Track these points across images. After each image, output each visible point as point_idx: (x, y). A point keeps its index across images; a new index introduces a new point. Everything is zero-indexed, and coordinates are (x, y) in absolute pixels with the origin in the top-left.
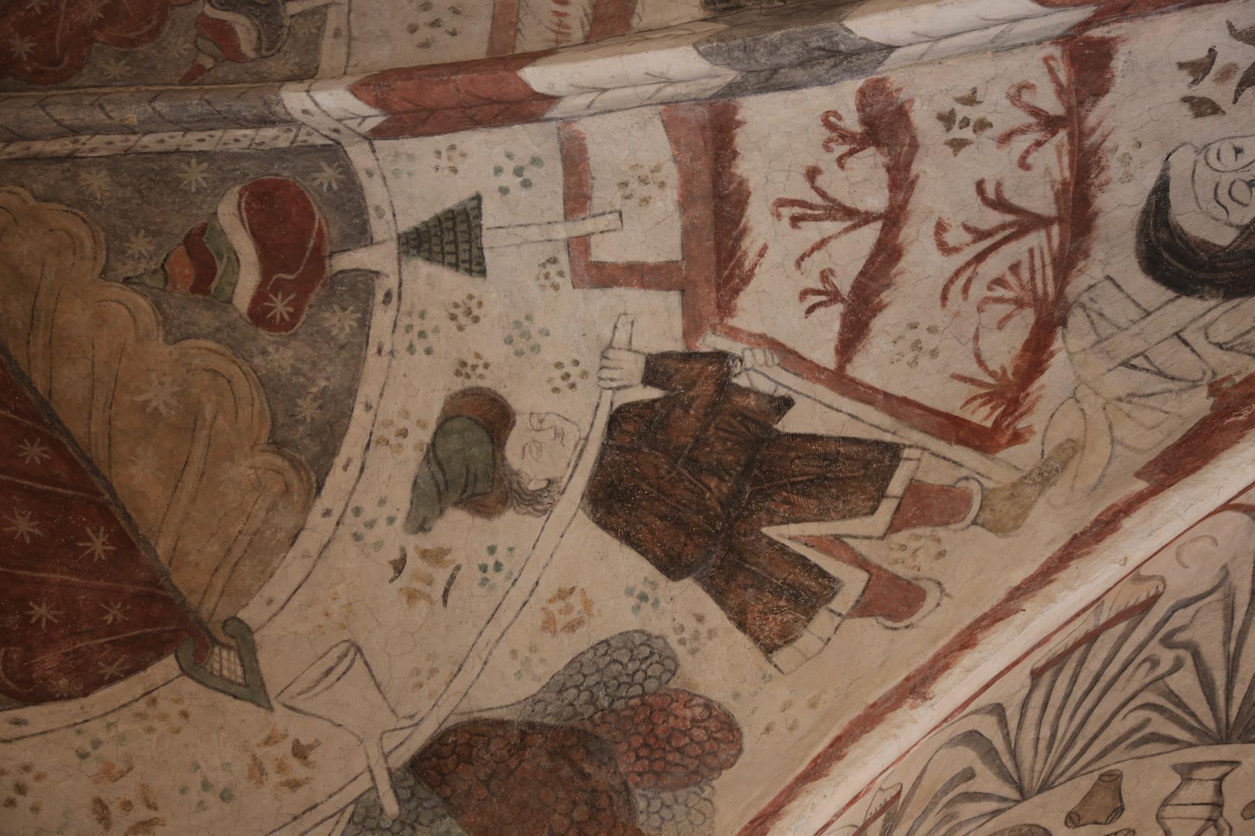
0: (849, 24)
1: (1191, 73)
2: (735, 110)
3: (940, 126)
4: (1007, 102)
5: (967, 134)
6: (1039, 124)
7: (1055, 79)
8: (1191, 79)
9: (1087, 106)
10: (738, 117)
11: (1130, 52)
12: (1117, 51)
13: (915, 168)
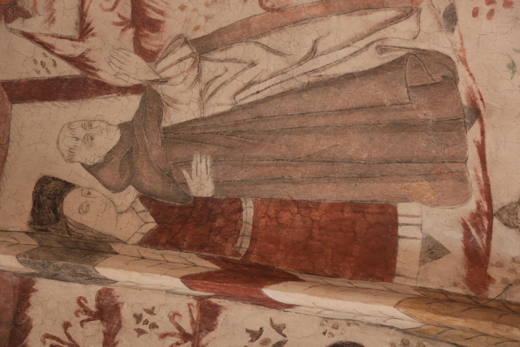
0: (97, 269)
1: (251, 336)
2: (33, 283)
3: (133, 320)
4: (167, 319)
5: (146, 328)
6: (180, 334)
7: (191, 316)
8: (250, 339)
9: (203, 334)
10: (34, 287)
11: (227, 315)
12: (221, 313)
13: (118, 337)
